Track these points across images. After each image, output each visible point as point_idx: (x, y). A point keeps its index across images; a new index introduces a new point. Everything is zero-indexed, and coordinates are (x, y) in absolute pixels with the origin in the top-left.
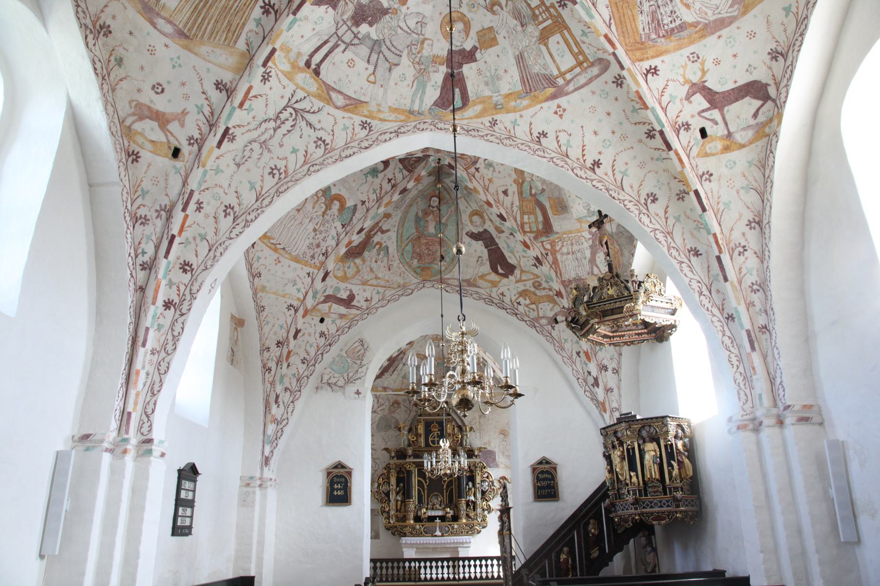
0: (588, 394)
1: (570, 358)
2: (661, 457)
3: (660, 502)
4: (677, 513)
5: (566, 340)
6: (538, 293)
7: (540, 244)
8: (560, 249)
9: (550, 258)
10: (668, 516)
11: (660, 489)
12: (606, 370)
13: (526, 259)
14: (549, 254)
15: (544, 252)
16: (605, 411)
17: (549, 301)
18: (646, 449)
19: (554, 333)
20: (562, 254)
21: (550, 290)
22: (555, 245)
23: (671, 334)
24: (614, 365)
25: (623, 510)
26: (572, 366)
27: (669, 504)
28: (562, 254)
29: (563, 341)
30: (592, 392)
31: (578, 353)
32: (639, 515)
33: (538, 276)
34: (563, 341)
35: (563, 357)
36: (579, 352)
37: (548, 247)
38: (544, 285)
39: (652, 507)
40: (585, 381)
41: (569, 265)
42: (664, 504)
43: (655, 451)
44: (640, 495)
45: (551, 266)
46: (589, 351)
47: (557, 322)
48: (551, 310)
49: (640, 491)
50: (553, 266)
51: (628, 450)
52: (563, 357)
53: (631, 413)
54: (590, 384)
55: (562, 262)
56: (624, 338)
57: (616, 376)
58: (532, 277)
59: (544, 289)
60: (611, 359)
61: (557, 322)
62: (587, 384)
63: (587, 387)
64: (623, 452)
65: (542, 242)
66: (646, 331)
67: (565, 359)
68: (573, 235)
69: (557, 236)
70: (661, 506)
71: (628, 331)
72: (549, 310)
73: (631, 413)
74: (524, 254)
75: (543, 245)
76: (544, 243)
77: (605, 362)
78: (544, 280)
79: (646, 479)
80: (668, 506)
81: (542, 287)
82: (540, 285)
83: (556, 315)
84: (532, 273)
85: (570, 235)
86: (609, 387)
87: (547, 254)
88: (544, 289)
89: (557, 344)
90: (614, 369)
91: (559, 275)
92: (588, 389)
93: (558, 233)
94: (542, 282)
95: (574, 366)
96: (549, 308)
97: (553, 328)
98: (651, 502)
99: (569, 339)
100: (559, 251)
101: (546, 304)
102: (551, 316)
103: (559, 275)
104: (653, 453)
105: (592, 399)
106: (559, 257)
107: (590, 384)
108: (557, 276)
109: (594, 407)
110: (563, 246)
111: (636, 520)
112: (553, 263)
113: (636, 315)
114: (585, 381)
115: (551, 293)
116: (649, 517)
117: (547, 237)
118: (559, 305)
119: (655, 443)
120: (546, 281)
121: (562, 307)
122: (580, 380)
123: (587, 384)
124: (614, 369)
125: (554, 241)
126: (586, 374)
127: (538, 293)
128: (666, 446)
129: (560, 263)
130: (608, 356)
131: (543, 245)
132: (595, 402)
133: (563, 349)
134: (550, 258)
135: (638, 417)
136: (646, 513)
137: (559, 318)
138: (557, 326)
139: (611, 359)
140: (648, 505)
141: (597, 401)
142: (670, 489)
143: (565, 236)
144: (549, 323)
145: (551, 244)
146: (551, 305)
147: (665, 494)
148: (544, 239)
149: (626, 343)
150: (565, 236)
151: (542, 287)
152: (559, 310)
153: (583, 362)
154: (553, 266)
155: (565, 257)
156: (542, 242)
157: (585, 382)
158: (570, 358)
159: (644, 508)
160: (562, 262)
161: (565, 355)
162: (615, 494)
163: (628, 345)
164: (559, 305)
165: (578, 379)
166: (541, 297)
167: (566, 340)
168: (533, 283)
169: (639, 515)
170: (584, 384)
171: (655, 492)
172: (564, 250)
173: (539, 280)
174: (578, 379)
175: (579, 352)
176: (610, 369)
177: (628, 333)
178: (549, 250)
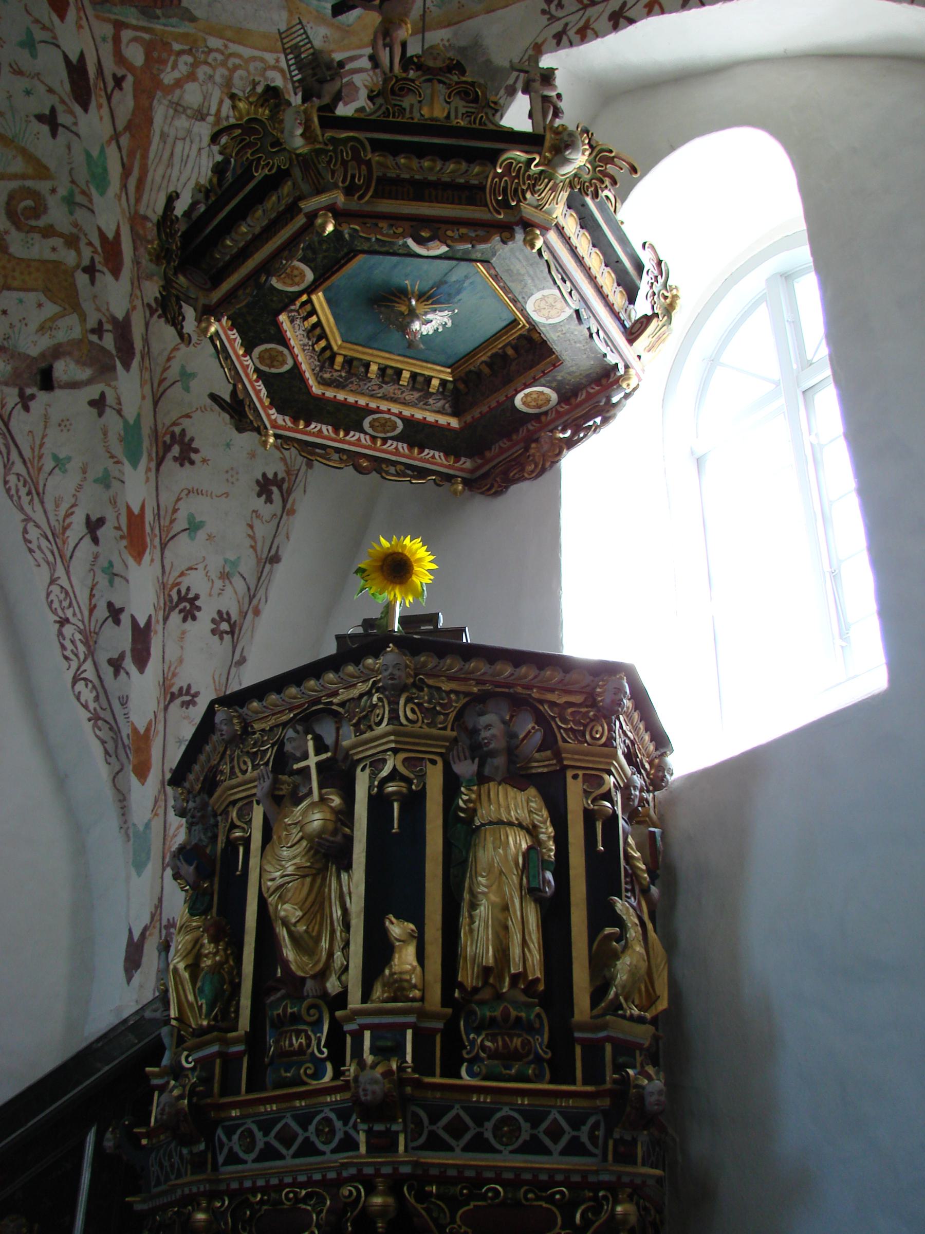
0: (88, 695)
1: (57, 535)
2: (561, 867)
3: (535, 1117)
4: (614, 1189)
5: (60, 463)
6: (17, 244)
7: (108, 30)
8: (179, 83)
9: (125, 102)
10: (568, 1208)
11: (540, 1043)
12: (190, 615)
13: (22, 83)
14: (128, 83)
15: (110, 66)
16: (142, 772)
17: (47, 291)
18: (486, 813)
19: (21, 423)
20: (178, 108)
21: (72, 242)
22: (164, 62)
23: (570, 444)
24: (230, 603)
25: (269, 1153)
26: (52, 567)
27: (584, 1135)
28: (178, 108)
29: (49, 464)
30: (101, 691)
31: (93, 526)
32: (395, 1185)
33: (42, 171)
34: (49, 464)
35: (28, 519)
36: (101, 521)
37: (136, 55)
38: (57, 215)
39: (479, 1145)
40: (90, 639)
41: (185, 162)
42: (555, 1133)
43: (532, 831)
44: (423, 1061)
45: (116, 137)
46: (149, 517)
47: (47, 381)
48: (42, 329)
49: (423, 1039)
50: (125, 140)
51: (378, 803)
52: (28, 519)
53: (433, 618)
54: (102, 658)
55: (164, 136)
56: (354, 436)
57: (221, 648)
58: (18, 165)
59: (48, 232)
60: (225, 576)
61: (47, 381)
62: (91, 653)
63: (88, 665)
64: (346, 815)
65: (119, 26)
66: (454, 423)
67: (33, 534)
68: (247, 52)
69: (186, 28)
70: (534, 1147)
71: (384, 398)
72: (33, 326)
73: (433, 618)
74: (23, 58)
75: (117, 40)
76: (126, 35)
77: (196, 583)
78: (62, 192)
79: (468, 976)
80: (574, 1148)
81: (41, 223)
82: (39, 210)
83: (57, 352)
84: (24, 152)
85: (234, 48)
86: (180, 682)
87: (119, 82)
88: (48, 232)
89: (19, 467)
90: (223, 616)
91: (132, 183)
92: (90, 674)
93: (193, 19)
94: (52, 202)
95: (60, 571)
96: (36, 318)
97: (25, 402)
98: (481, 1115)
99: (74, 466)
100: (168, 90)
101: (31, 298)
102: (34, 352)
103: (132, 183)
104: (519, 842)
105: (95, 718)
106: (160, 112)
107: (102, 658)
108: (124, 186)
109: (97, 750)
110: (191, 77)
111: (365, 1219)
112: (129, 127)
113: (528, 226)
114: (90, 639)
115: (69, 257)
116: (455, 1203)
117: (146, 12)
118: (83, 318)
119: (532, 791)
120: (70, 202)
121: (92, 323)
122: (68, 630)
123: (91, 653)
124: (223, 616)
125: (166, 45)
126: (102, 612)
127: (17, 244)
128: (589, 817)
129: (156, 140)
130: (215, 564)
131: (117, 40)
132: (105, 734)
133: (37, 492)
134: (125, 102)
135: (467, 638)
136: (442, 1179)
137: (63, 369)
138: (43, 397)
139: (225, 576)
140: (456, 1128)
141: (115, 730)
142: (593, 1050)
143: (214, 42)
144: (15, 379)
145: (149, 49)
146: (51, 309)
147: (562, 1073)
148: (132, 16)
149: (352, 459)
150: (214, 42)
151: (41, 223)
152: (77, 333)
153: (103, 562)
154: (125, 140)
155: (182, 122)
156: (119, 26)
157: (86, 643)
158: (57, 535)
159: (435, 1144)
160: (164, 136)
161: (39, 516)
162: (230, 1062)
163: (359, 470)
164: (83, 318)
165: (63, 622)
166: (27, 263)
167: (60, 463)
168: (11, 197)
169: (395, 1185)
170: (82, 649)
171: (508, 1056)
172: (192, 95)
173: (43, 186)
174: (63, 622)
175: (101, 521)
176: (205, 616)
177: (384, 406)
178: (130, 68)
